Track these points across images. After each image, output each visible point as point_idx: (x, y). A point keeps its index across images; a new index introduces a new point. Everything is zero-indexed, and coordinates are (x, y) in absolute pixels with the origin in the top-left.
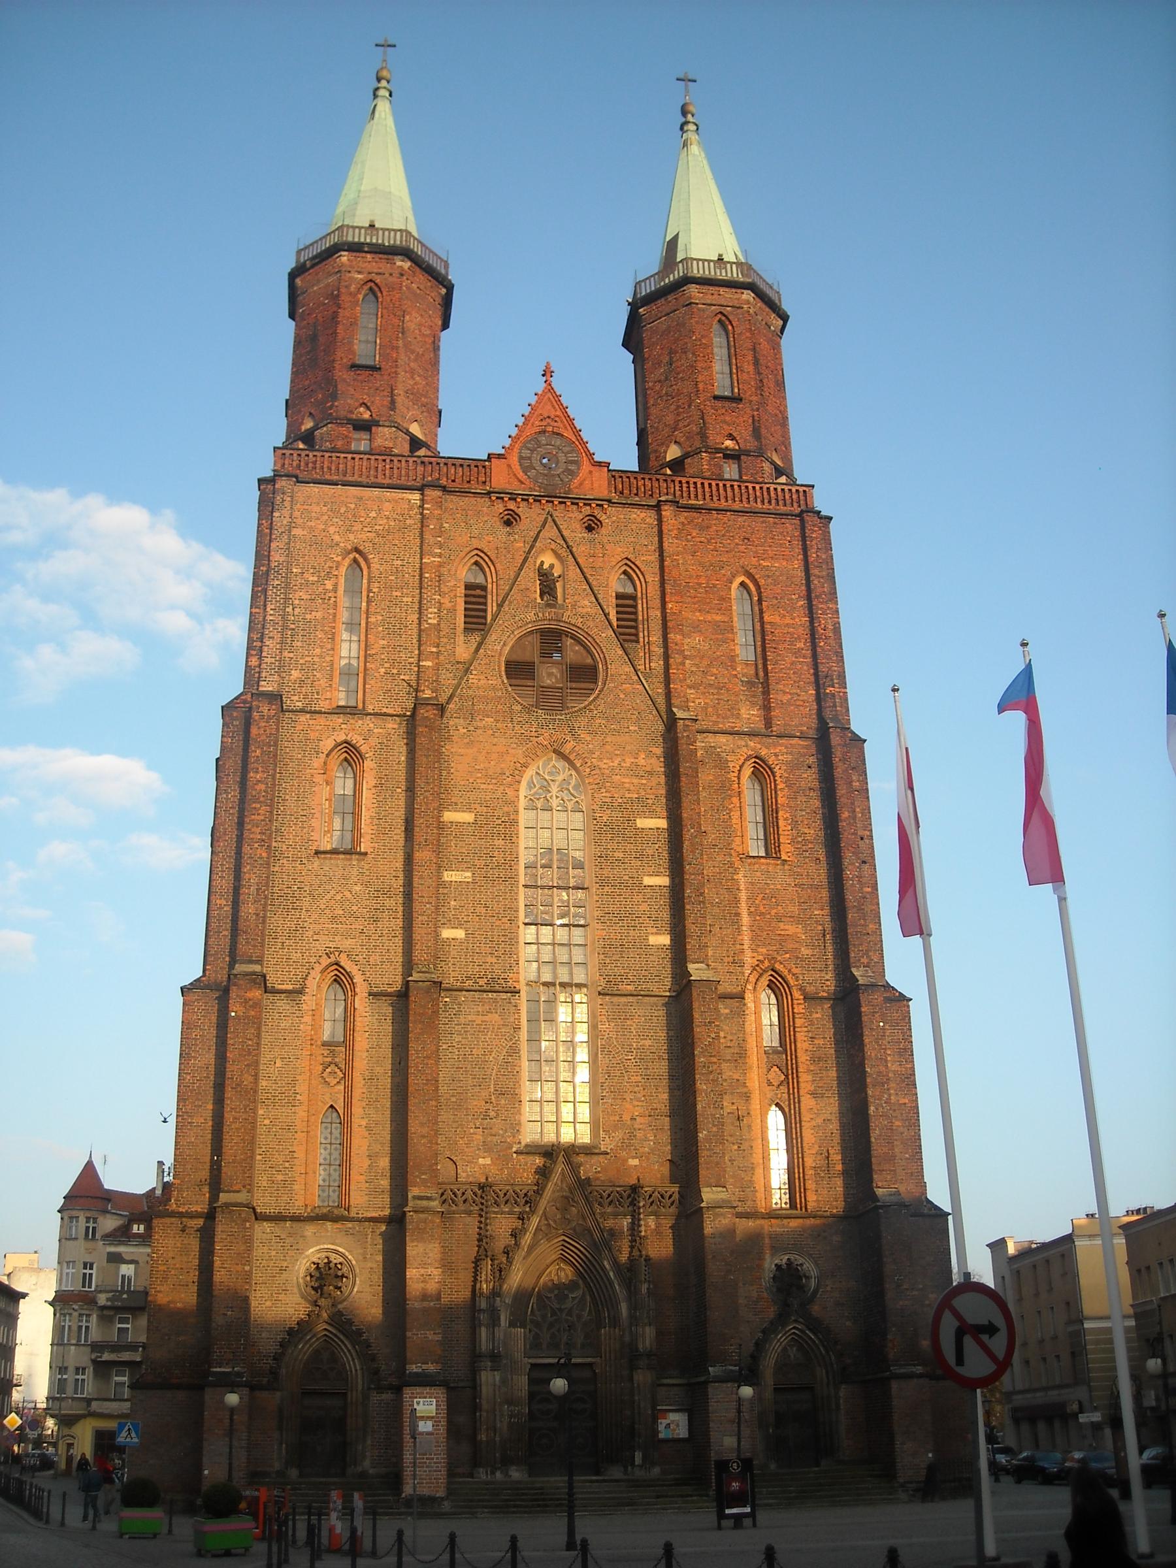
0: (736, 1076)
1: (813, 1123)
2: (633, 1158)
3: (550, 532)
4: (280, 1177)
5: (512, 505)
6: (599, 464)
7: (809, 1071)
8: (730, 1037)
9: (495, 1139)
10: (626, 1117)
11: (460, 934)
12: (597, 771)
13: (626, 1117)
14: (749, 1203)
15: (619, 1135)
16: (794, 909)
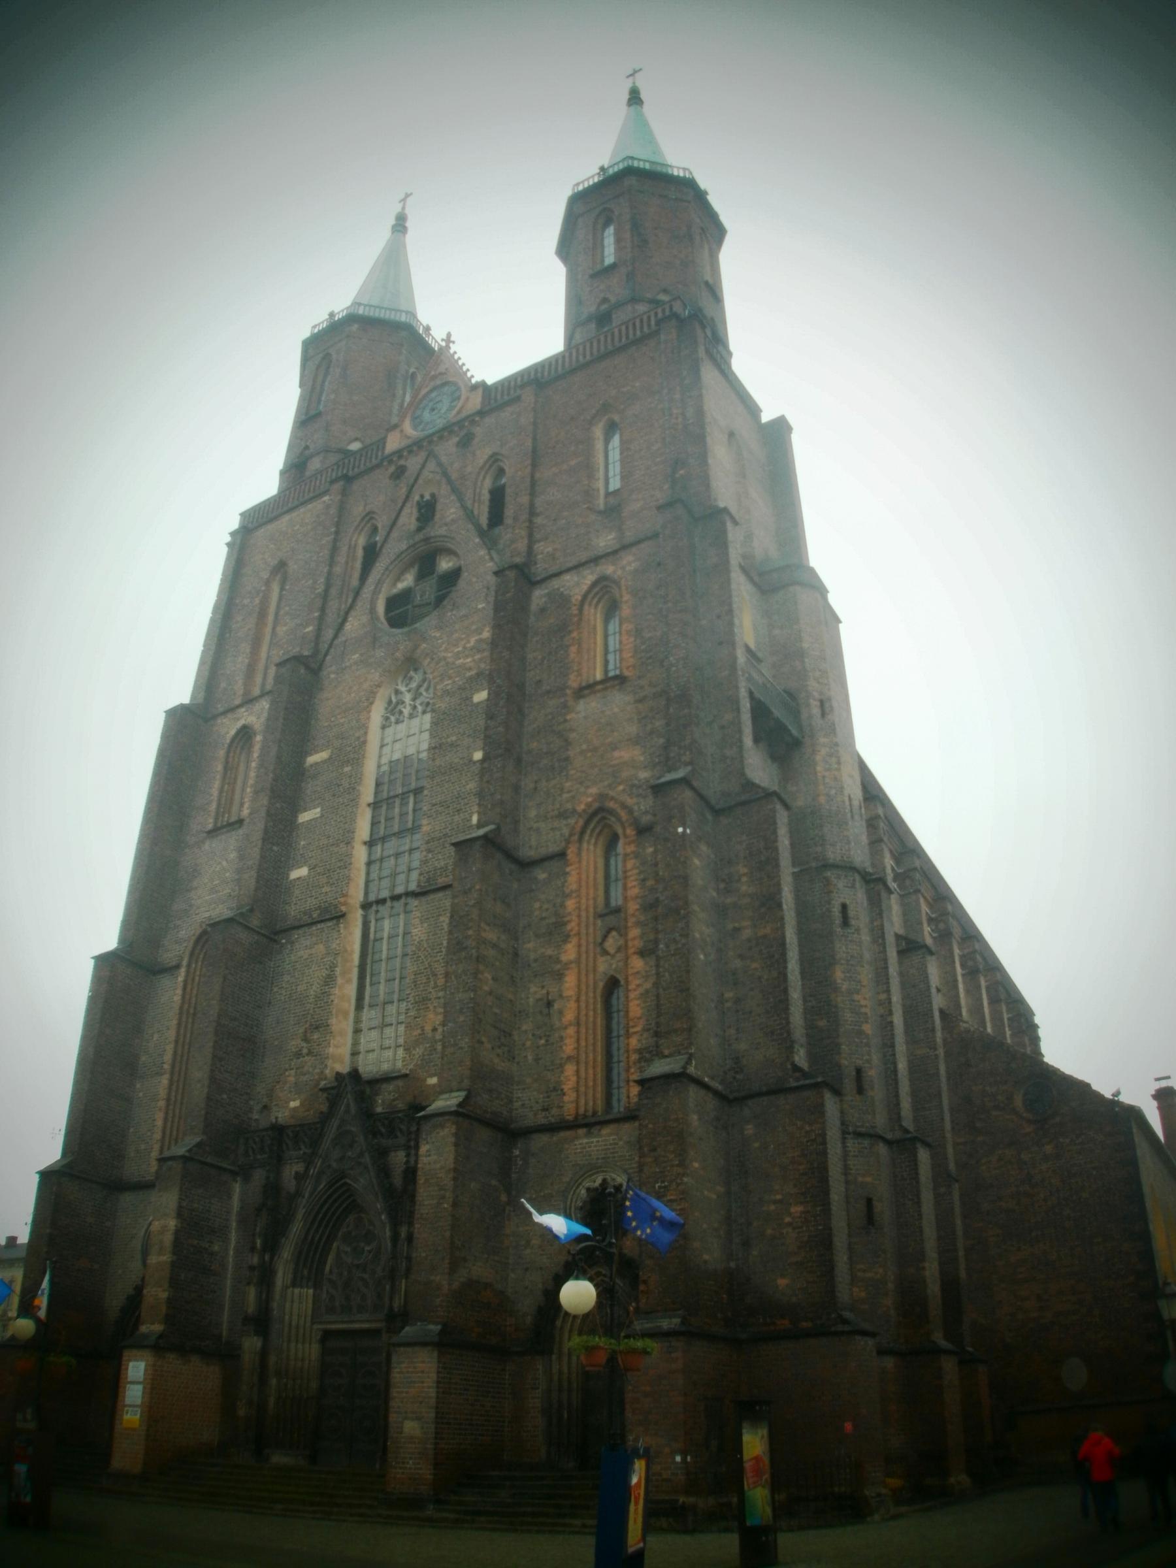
0: (549, 952)
1: (641, 990)
2: (432, 1076)
3: (432, 465)
4: (143, 1147)
5: (402, 462)
6: (475, 387)
7: (638, 924)
8: (545, 906)
9: (305, 1078)
10: (428, 1028)
11: (303, 872)
12: (443, 663)
13: (428, 1028)
14: (554, 1111)
15: (418, 1051)
16: (633, 729)
